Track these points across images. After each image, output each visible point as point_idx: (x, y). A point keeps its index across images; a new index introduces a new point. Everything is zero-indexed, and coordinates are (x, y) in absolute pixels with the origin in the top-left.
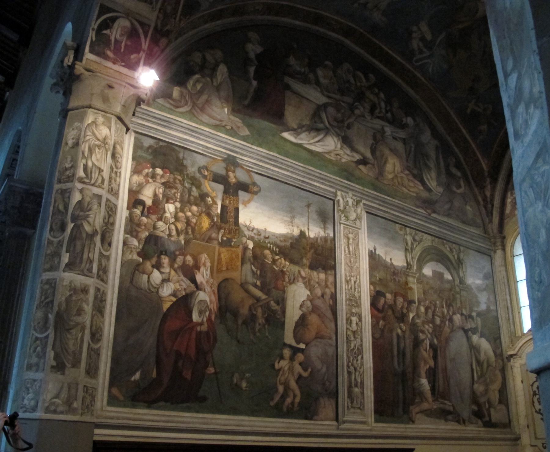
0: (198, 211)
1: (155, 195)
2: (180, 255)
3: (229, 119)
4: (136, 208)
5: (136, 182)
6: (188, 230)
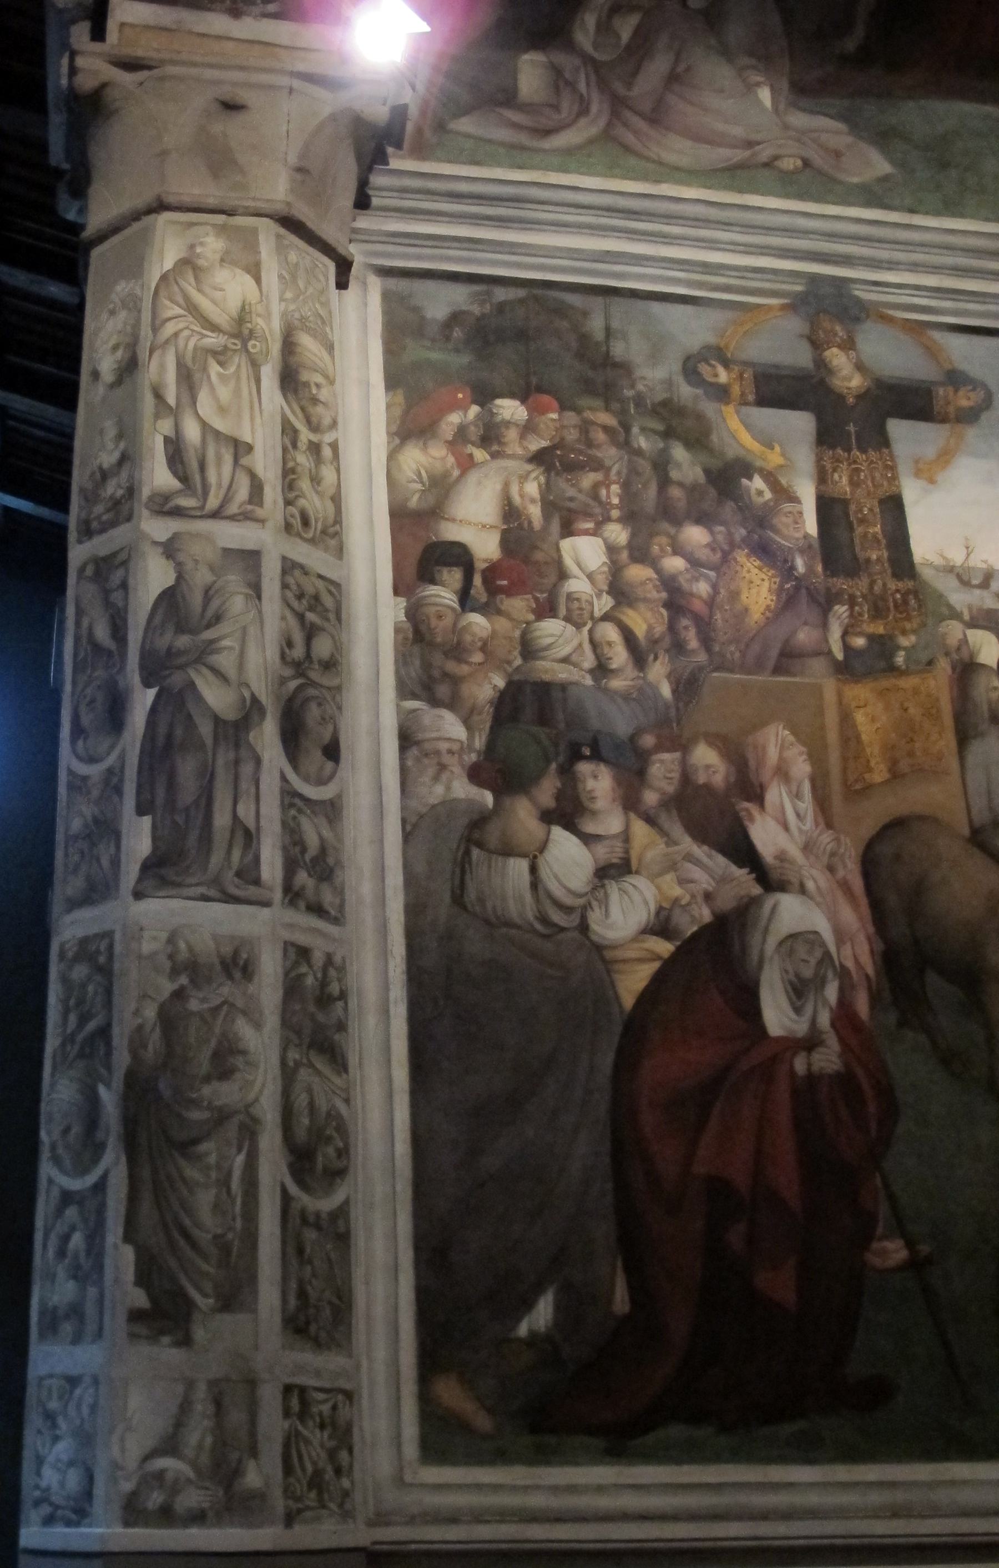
0: (712, 547)
1: (510, 513)
2: (659, 748)
3: (786, 127)
4: (433, 581)
5: (419, 474)
6: (683, 634)
